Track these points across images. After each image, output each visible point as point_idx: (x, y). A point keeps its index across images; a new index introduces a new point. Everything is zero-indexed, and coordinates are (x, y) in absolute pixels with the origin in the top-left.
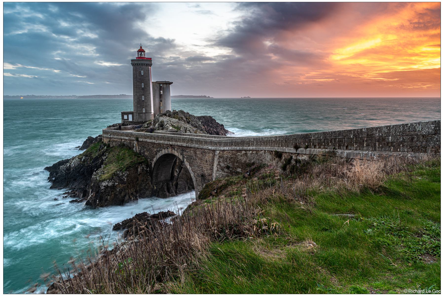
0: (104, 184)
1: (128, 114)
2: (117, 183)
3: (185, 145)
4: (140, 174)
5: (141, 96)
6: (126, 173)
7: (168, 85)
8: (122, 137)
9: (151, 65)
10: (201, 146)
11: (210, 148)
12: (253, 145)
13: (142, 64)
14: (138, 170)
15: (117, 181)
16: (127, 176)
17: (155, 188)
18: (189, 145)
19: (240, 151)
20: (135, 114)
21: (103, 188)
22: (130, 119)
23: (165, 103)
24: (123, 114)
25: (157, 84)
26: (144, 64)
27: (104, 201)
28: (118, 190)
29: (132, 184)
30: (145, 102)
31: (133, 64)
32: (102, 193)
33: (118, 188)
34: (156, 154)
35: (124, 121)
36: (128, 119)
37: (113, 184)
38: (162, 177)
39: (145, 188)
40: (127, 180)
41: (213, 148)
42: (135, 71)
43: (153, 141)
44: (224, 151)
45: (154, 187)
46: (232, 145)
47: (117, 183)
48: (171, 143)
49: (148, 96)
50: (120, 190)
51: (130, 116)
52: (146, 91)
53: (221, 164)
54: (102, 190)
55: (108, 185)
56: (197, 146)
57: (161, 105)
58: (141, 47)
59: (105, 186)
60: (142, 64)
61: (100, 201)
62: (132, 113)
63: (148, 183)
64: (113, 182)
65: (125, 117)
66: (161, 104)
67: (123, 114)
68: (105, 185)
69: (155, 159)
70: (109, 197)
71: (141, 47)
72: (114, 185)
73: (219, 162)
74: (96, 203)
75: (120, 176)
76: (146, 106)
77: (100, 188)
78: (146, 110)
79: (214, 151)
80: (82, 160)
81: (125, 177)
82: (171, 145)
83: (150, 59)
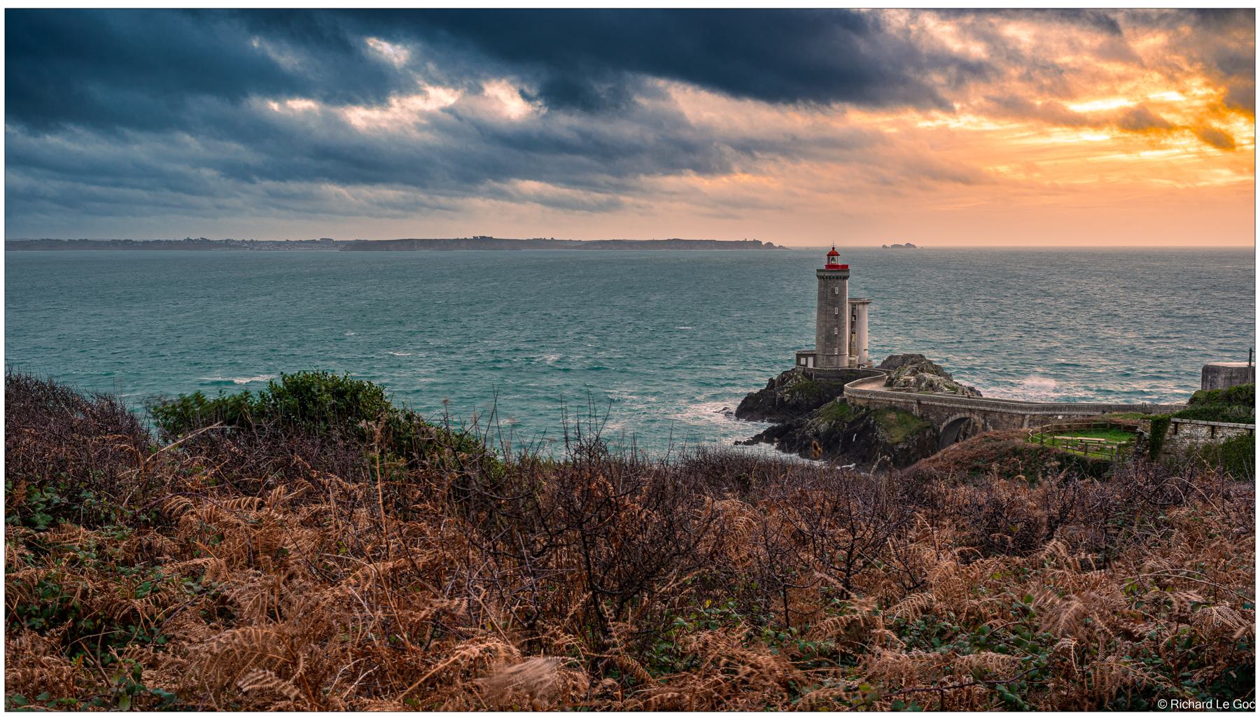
1: (806, 356)
3: (988, 409)
5: (832, 327)
6: (916, 437)
8: (893, 399)
9: (846, 278)
12: (1065, 410)
18: (994, 409)
19: (1052, 415)
20: (820, 357)
22: (810, 366)
23: (859, 337)
34: (948, 418)
36: (806, 365)
41: (1023, 412)
44: (1035, 415)
48: (970, 407)
51: (811, 360)
56: (1003, 410)
57: (853, 340)
58: (833, 248)
65: (803, 361)
67: (799, 356)
69: (945, 424)
72: (908, 448)
76: (840, 344)
78: (839, 351)
79: (1024, 415)
83: (845, 268)
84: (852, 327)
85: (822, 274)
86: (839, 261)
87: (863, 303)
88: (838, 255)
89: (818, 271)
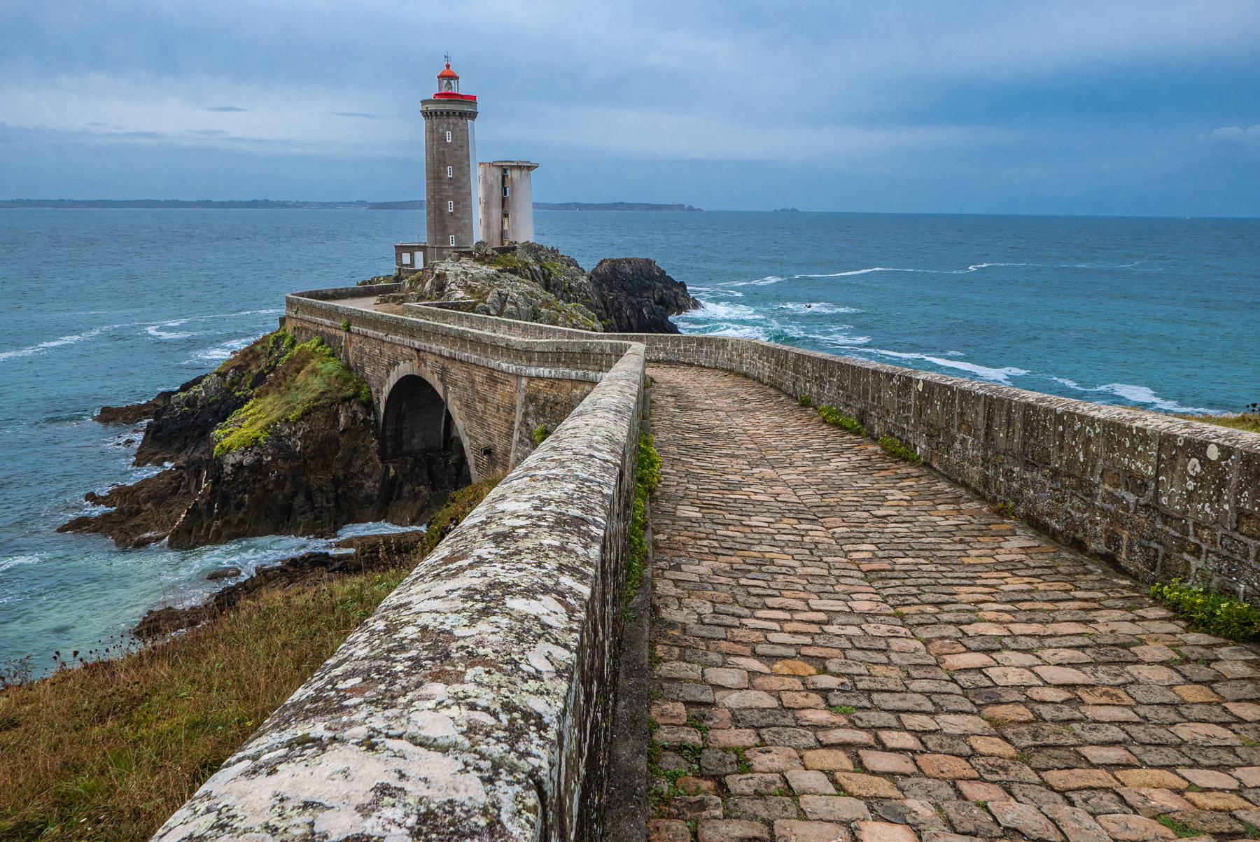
0: (230, 459)
1: (411, 249)
2: (270, 458)
4: (344, 431)
7: (525, 172)
9: (473, 116)
10: (483, 359)
11: (504, 366)
13: (448, 113)
14: (338, 420)
15: (270, 451)
16: (304, 438)
17: (392, 472)
21: (228, 469)
23: (514, 221)
24: (400, 249)
25: (494, 169)
26: (454, 113)
27: (232, 507)
28: (272, 476)
29: (322, 460)
30: (456, 218)
31: (426, 114)
32: (228, 483)
33: (273, 473)
35: (400, 270)
36: (412, 264)
37: (258, 460)
38: (415, 441)
39: (362, 471)
40: (305, 448)
42: (431, 131)
43: (381, 334)
44: (539, 378)
45: (387, 469)
46: (559, 361)
47: (270, 458)
48: (417, 344)
49: (465, 200)
50: (278, 476)
51: (419, 256)
52: (459, 188)
53: (530, 421)
54: (228, 475)
55: (241, 463)
57: (506, 228)
58: (448, 66)
59: (233, 465)
60: (448, 113)
61: (221, 507)
62: (423, 248)
63: (371, 459)
64: (256, 454)
65: (406, 258)
66: (506, 223)
68: (234, 462)
69: (386, 390)
70: (247, 496)
71: (448, 66)
73: (526, 414)
74: (212, 511)
75: (285, 436)
77: (223, 469)
80: (228, 379)
81: (299, 439)
82: (418, 351)
83: (471, 100)
84: (503, 207)
85: (431, 107)
86: (462, 88)
87: (520, 168)
88: (455, 78)
89: (424, 102)
